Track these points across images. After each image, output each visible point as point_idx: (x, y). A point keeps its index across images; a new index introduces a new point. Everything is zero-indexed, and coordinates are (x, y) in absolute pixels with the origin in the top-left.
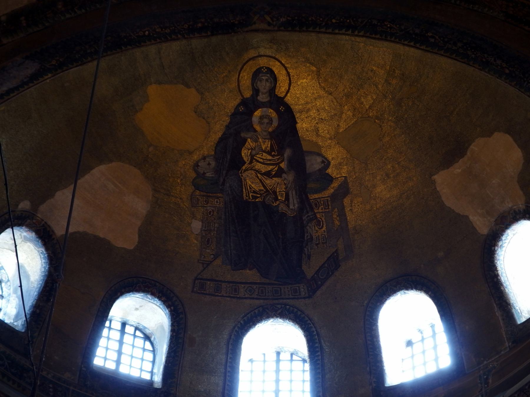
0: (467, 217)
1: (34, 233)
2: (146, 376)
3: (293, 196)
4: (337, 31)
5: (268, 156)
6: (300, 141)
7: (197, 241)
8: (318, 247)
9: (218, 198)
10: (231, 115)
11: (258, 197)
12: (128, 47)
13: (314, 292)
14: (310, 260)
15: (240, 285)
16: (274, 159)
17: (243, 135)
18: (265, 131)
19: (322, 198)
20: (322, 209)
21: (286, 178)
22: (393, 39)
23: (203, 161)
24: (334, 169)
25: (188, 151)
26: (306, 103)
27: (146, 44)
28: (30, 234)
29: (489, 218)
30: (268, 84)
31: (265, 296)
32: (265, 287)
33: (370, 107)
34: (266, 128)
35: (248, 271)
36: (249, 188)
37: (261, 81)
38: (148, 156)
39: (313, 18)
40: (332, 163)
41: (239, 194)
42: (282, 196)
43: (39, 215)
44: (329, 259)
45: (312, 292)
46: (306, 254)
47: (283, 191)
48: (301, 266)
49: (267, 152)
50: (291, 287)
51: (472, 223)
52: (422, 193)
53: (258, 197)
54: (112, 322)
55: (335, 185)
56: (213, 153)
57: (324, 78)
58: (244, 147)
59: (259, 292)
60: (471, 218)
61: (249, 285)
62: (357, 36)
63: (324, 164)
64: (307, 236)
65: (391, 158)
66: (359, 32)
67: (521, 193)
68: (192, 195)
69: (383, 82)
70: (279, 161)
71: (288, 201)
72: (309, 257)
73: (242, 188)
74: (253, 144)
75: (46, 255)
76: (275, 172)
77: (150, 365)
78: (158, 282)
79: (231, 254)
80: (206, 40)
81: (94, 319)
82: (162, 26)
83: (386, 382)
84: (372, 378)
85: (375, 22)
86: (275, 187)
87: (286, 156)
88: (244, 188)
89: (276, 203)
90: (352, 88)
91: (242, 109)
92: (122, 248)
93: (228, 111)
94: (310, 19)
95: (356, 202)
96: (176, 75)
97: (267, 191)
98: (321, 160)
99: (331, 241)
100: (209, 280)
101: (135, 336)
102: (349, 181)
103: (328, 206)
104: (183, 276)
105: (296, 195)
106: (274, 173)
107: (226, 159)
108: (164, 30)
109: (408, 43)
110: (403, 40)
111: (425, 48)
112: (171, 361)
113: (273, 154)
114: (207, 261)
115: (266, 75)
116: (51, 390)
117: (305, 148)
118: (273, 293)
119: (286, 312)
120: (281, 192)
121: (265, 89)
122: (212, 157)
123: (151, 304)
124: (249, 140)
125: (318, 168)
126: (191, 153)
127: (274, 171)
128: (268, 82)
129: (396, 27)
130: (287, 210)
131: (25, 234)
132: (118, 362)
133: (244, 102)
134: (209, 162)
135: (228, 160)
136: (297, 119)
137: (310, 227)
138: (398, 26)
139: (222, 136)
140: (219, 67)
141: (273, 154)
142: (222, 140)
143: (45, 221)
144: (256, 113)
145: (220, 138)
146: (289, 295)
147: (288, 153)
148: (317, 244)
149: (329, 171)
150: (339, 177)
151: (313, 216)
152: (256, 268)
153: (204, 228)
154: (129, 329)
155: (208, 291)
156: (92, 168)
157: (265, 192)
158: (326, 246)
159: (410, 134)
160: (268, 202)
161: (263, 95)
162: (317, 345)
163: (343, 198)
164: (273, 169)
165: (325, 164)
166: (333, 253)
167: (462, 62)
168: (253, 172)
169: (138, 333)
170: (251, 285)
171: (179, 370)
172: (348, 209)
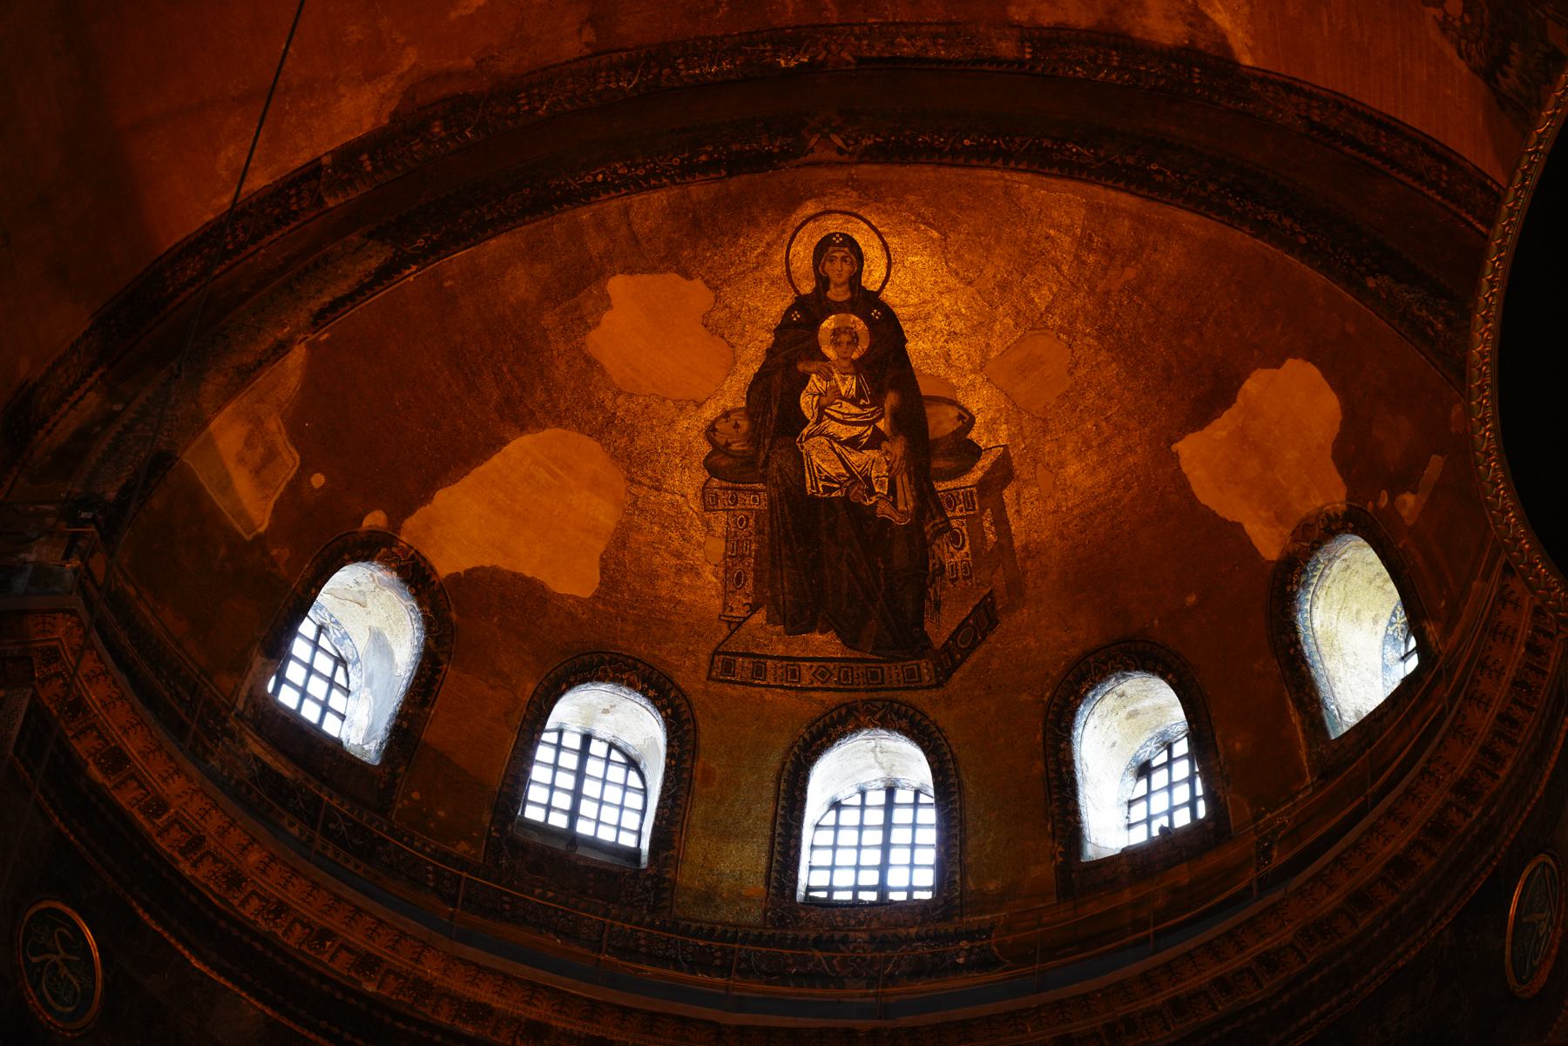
0: (1240, 526)
1: (395, 574)
2: (628, 841)
5: (852, 406)
6: (914, 377)
7: (716, 577)
9: (756, 492)
10: (775, 330)
11: (835, 489)
12: (565, 206)
13: (948, 674)
15: (801, 663)
17: (801, 367)
18: (846, 358)
19: (961, 488)
20: (961, 511)
22: (1084, 176)
23: (723, 420)
24: (982, 431)
25: (695, 402)
26: (923, 302)
28: (388, 574)
29: (1280, 528)
30: (846, 267)
31: (852, 684)
32: (852, 668)
33: (1048, 310)
34: (845, 353)
35: (818, 636)
37: (831, 261)
38: (615, 414)
39: (927, 138)
40: (979, 420)
41: (798, 484)
42: (882, 485)
43: (403, 538)
44: (976, 608)
45: (944, 675)
47: (884, 476)
50: (902, 667)
51: (1249, 537)
52: (1153, 477)
53: (835, 489)
54: (565, 735)
55: (985, 462)
56: (744, 404)
57: (955, 252)
58: (805, 391)
59: (839, 678)
60: (1247, 527)
61: (820, 664)
62: (1014, 170)
63: (963, 422)
64: (934, 565)
65: (1093, 410)
67: (1339, 479)
68: (704, 488)
69: (1070, 259)
71: (895, 497)
72: (938, 605)
74: (822, 384)
75: (420, 615)
77: (637, 817)
78: (640, 661)
79: (784, 603)
80: (719, 184)
81: (516, 736)
82: (629, 162)
83: (1082, 854)
84: (1056, 845)
85: (1047, 143)
88: (807, 470)
89: (871, 500)
90: (1011, 273)
91: (797, 316)
92: (569, 596)
93: (770, 321)
94: (920, 139)
95: (1026, 496)
96: (662, 255)
98: (957, 414)
100: (742, 655)
101: (608, 761)
102: (1012, 455)
103: (974, 504)
104: (690, 649)
105: (910, 483)
106: (865, 440)
107: (769, 416)
109: (1114, 182)
111: (1146, 193)
112: (666, 815)
113: (861, 403)
116: (430, 876)
117: (924, 392)
118: (867, 679)
119: (893, 715)
121: (840, 276)
122: (742, 413)
123: (629, 704)
125: (951, 430)
126: (699, 405)
128: (846, 261)
129: (1087, 154)
130: (893, 514)
131: (379, 574)
132: (573, 814)
133: (801, 302)
137: (939, 546)
138: (1092, 151)
139: (760, 369)
140: (748, 236)
141: (861, 403)
142: (758, 377)
143: (415, 548)
144: (825, 324)
145: (756, 375)
146: (899, 681)
147: (891, 400)
148: (953, 581)
149: (973, 435)
150: (993, 447)
151: (944, 525)
153: (730, 553)
154: (597, 748)
156: (505, 442)
157: (849, 479)
158: (970, 584)
159: (1128, 363)
161: (838, 289)
162: (951, 781)
163: (1002, 489)
164: (863, 434)
165: (965, 421)
166: (985, 597)
167: (1219, 221)
168: (823, 439)
169: (615, 755)
171: (681, 832)
172: (1013, 511)
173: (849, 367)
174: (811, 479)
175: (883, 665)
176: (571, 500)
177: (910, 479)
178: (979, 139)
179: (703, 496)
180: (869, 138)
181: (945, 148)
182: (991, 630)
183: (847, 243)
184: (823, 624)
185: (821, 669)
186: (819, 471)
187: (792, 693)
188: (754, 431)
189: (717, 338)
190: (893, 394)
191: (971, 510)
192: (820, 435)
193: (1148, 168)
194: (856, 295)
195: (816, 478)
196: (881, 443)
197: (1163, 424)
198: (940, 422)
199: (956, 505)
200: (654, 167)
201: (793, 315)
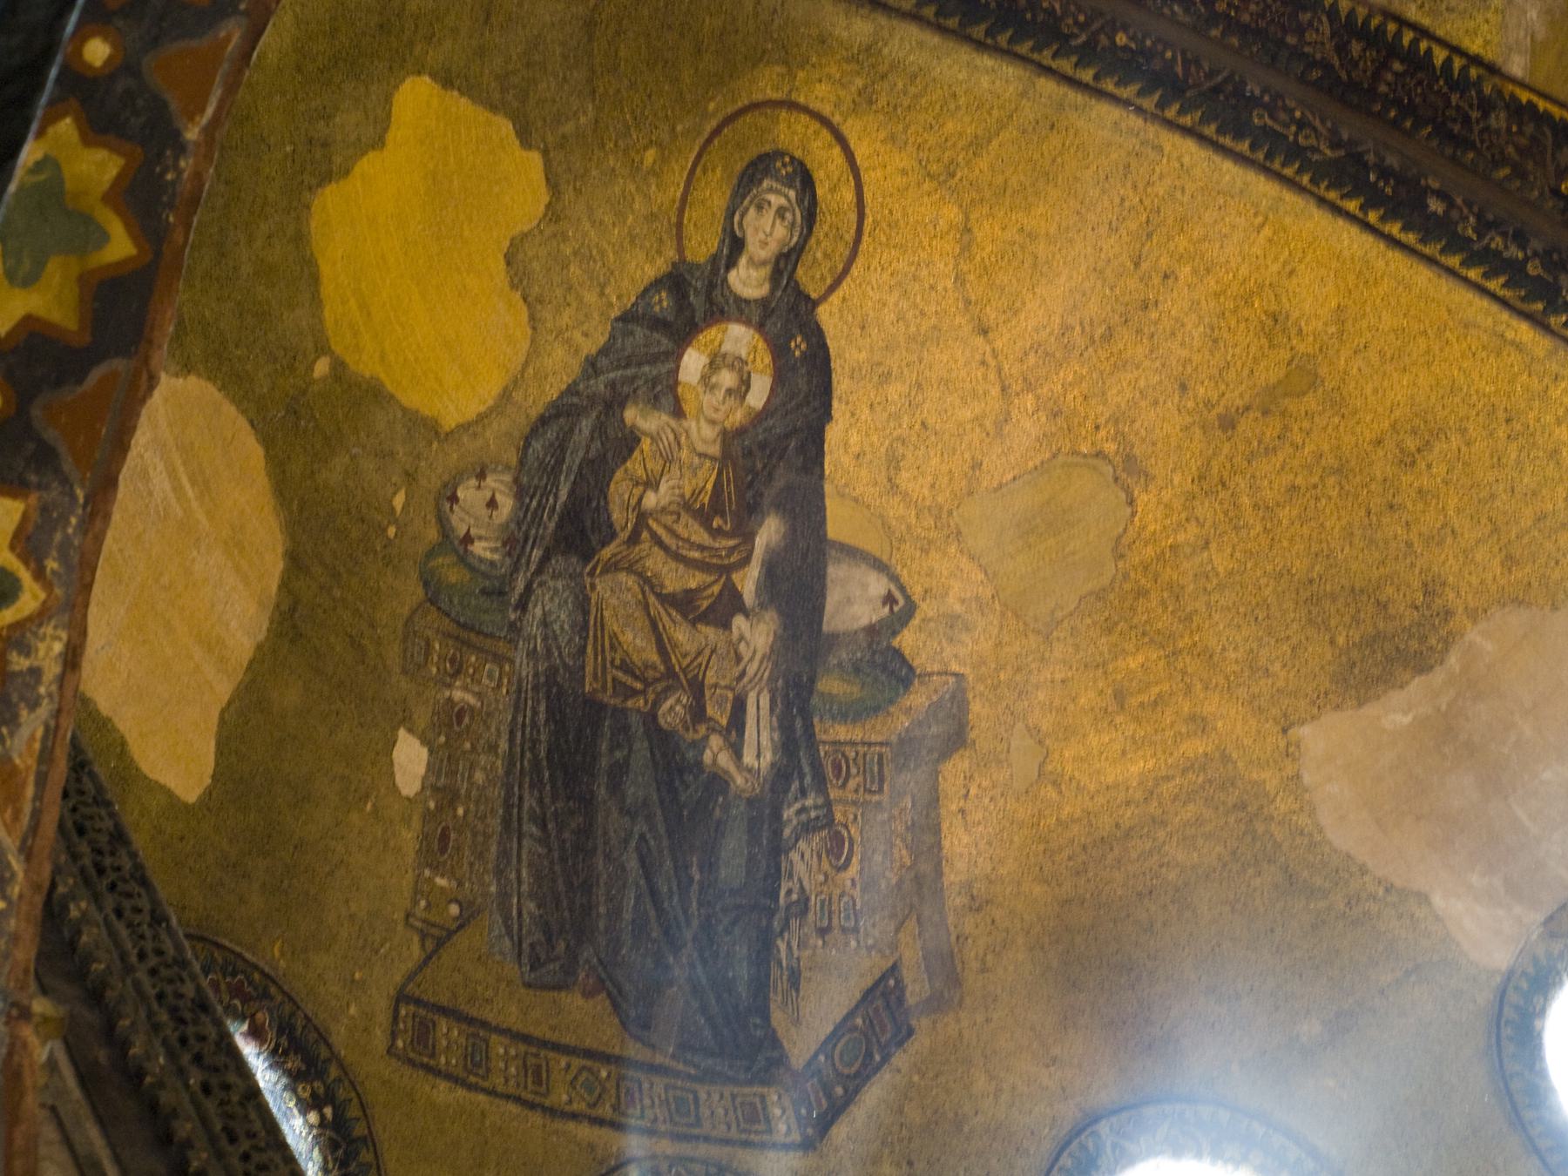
4: (1109, 85)
5: (696, 526)
9: (499, 659)
10: (617, 319)
14: (797, 990)
15: (551, 1055)
17: (631, 414)
18: (713, 422)
19: (864, 743)
21: (747, 635)
22: (1289, 172)
23: (473, 482)
29: (1518, 910)
35: (580, 1001)
37: (760, 208)
39: (1057, 6)
40: (926, 609)
46: (784, 965)
50: (734, 1097)
55: (918, 698)
62: (1171, 125)
63: (891, 609)
64: (789, 892)
66: (1181, 112)
72: (795, 979)
86: (700, 665)
87: (760, 542)
97: (670, 673)
98: (883, 592)
105: (772, 710)
106: (705, 604)
107: (551, 500)
110: (1326, 183)
113: (715, 525)
114: (433, 925)
117: (834, 530)
121: (764, 244)
124: (646, 444)
125: (864, 622)
130: (732, 769)
133: (675, 281)
134: (493, 496)
136: (835, 404)
137: (803, 856)
139: (562, 395)
149: (907, 640)
152: (604, 995)
155: (443, 1060)
158: (853, 944)
164: (705, 588)
166: (883, 978)
170: (588, 1063)
173: (715, 441)
174: (596, 659)
175: (697, 1086)
176: (194, 560)
177: (773, 702)
178: (1143, 41)
179: (405, 639)
181: (1076, 36)
182: (900, 1044)
187: (536, 1118)
188: (519, 524)
189: (517, 296)
190: (777, 521)
192: (630, 570)
193: (1423, 182)
194: (779, 293)
195: (604, 659)
196: (732, 615)
197: (1280, 684)
198: (849, 601)
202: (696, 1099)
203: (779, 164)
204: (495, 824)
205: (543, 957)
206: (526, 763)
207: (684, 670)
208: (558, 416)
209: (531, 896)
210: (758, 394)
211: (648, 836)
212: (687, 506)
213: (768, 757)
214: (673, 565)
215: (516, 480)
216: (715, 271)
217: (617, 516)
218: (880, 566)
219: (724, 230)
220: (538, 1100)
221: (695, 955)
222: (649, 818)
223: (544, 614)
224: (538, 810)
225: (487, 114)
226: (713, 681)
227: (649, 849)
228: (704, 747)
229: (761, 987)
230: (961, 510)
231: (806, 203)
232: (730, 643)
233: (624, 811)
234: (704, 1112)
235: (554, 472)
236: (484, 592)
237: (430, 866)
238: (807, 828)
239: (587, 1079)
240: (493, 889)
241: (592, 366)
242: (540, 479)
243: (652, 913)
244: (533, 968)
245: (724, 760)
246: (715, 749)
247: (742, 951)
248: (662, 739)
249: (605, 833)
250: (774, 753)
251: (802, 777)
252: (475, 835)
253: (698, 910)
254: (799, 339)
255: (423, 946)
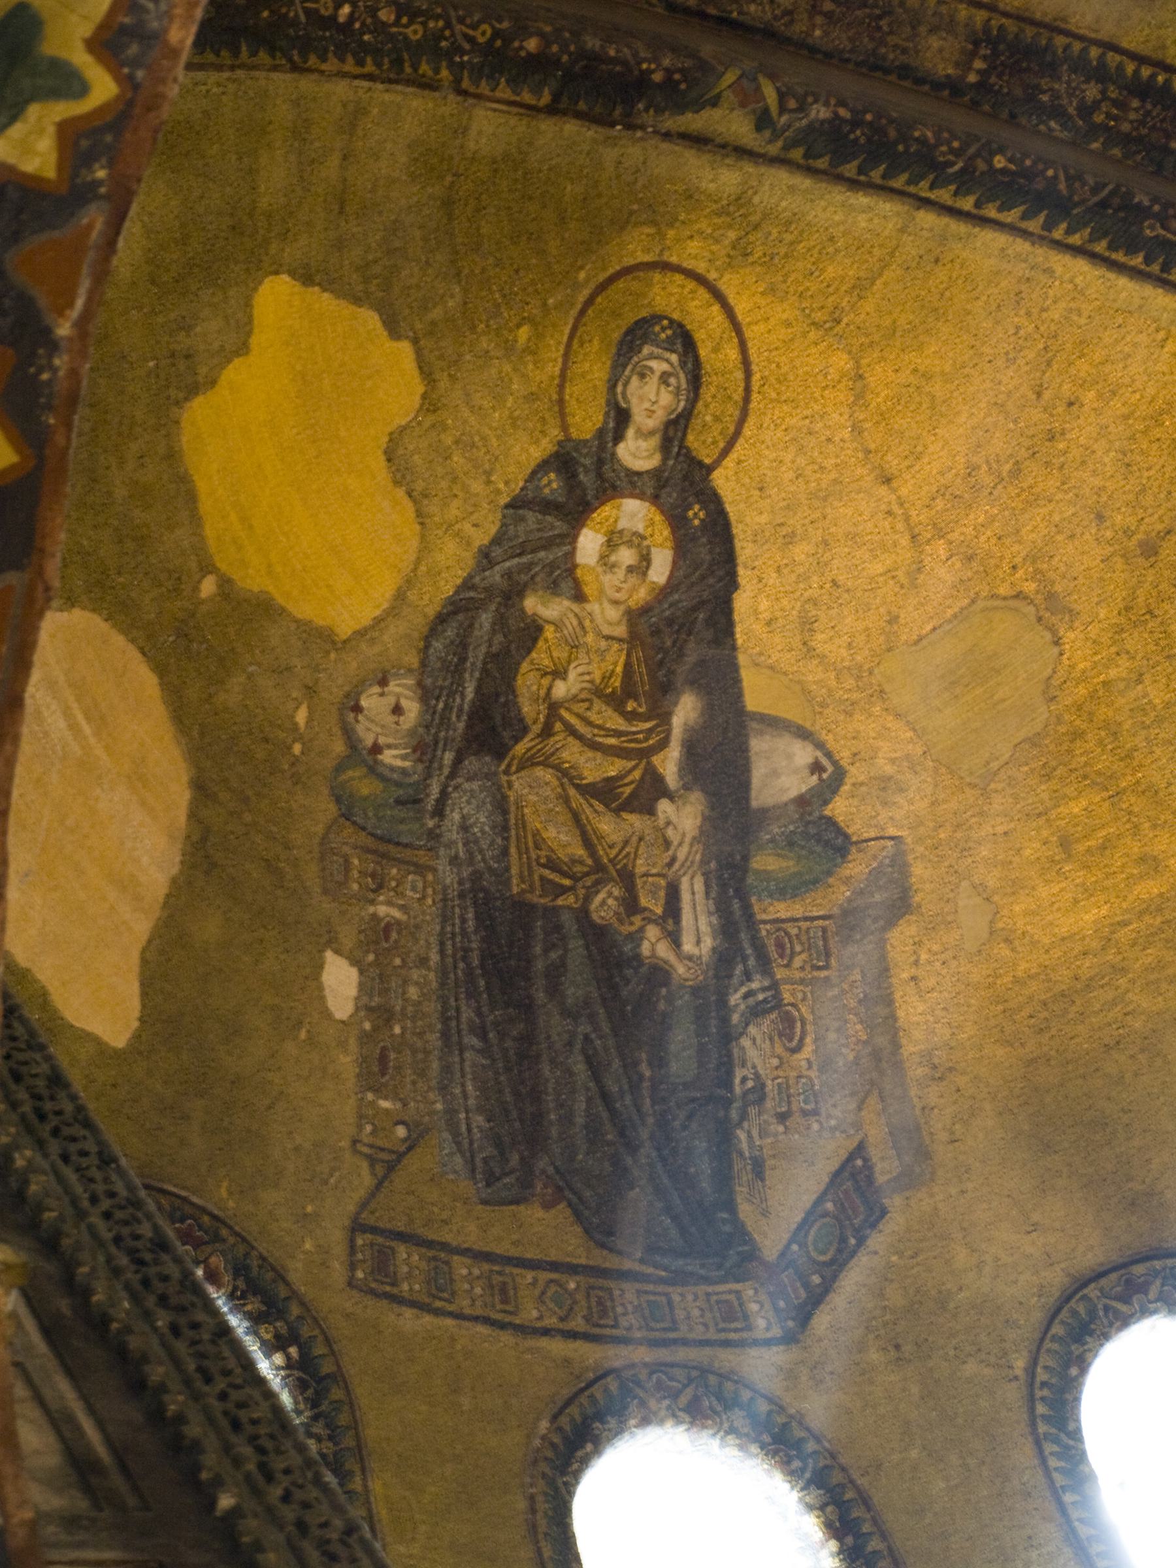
3: (694, 900)
4: (991, 212)
8: (786, 1127)
9: (420, 870)
10: (507, 506)
11: (564, 890)
14: (763, 1180)
15: (516, 1271)
16: (634, 729)
17: (531, 604)
18: (616, 603)
19: (806, 919)
21: (674, 819)
23: (376, 689)
27: (324, 67)
34: (619, 590)
35: (540, 1213)
36: (531, 844)
37: (642, 376)
39: (929, 134)
40: (856, 773)
46: (747, 1154)
48: (730, 1206)
49: (606, 696)
53: (564, 890)
55: (857, 867)
63: (820, 779)
64: (744, 1080)
66: (1069, 232)
70: (651, 742)
72: (759, 1169)
73: (507, 839)
76: (633, 786)
79: (469, 1130)
89: (632, 924)
94: (917, 134)
97: (599, 867)
98: (810, 760)
99: (834, 1106)
105: (707, 893)
106: (628, 790)
107: (458, 700)
108: (405, 20)
114: (382, 1149)
115: (667, 355)
117: (751, 703)
119: (715, 1403)
120: (650, 879)
124: (549, 632)
125: (793, 793)
127: (626, 785)
135: (466, 707)
136: (741, 571)
151: (769, 993)
158: (816, 1126)
160: (603, 914)
165: (825, 776)
166: (851, 1158)
173: (619, 623)
175: (670, 1289)
178: (1023, 161)
179: (322, 859)
180: (827, 104)
181: (953, 164)
182: (873, 1226)
183: (679, 347)
184: (545, 1187)
185: (553, 1288)
186: (537, 847)
189: (401, 493)
191: (819, 968)
192: (545, 764)
194: (671, 462)
198: (775, 773)
199: (793, 954)
200: (442, 30)
201: (545, 481)
202: (670, 1303)
203: (657, 328)
204: (434, 1038)
205: (497, 1171)
206: (460, 973)
207: (611, 861)
208: (455, 613)
209: (480, 1109)
210: (660, 570)
211: (593, 1036)
212: (598, 692)
213: (708, 943)
214: (590, 754)
215: (420, 684)
216: (602, 447)
217: (527, 709)
218: (804, 734)
219: (608, 403)
220: (508, 1319)
221: (654, 1154)
222: (592, 1017)
223: (463, 817)
224: (478, 1021)
225: (353, 308)
226: (643, 869)
227: (595, 1049)
228: (642, 939)
229: (724, 1179)
230: (881, 667)
231: (690, 365)
232: (657, 829)
233: (566, 1013)
234: (680, 1314)
235: (457, 671)
236: (399, 802)
237: (370, 1089)
238: (756, 1012)
239: (556, 1292)
240: (439, 1106)
241: (486, 557)
242: (445, 679)
243: (605, 1115)
244: (488, 1185)
245: (663, 950)
246: (653, 940)
247: (701, 1145)
248: (596, 934)
249: (549, 1037)
250: (714, 939)
251: (745, 959)
252: (414, 1052)
253: (653, 1106)
254: (697, 507)
255: (373, 1174)
